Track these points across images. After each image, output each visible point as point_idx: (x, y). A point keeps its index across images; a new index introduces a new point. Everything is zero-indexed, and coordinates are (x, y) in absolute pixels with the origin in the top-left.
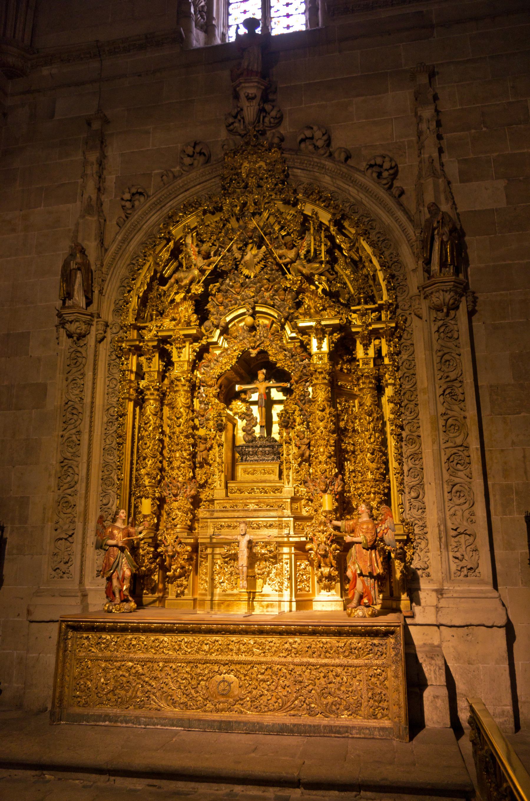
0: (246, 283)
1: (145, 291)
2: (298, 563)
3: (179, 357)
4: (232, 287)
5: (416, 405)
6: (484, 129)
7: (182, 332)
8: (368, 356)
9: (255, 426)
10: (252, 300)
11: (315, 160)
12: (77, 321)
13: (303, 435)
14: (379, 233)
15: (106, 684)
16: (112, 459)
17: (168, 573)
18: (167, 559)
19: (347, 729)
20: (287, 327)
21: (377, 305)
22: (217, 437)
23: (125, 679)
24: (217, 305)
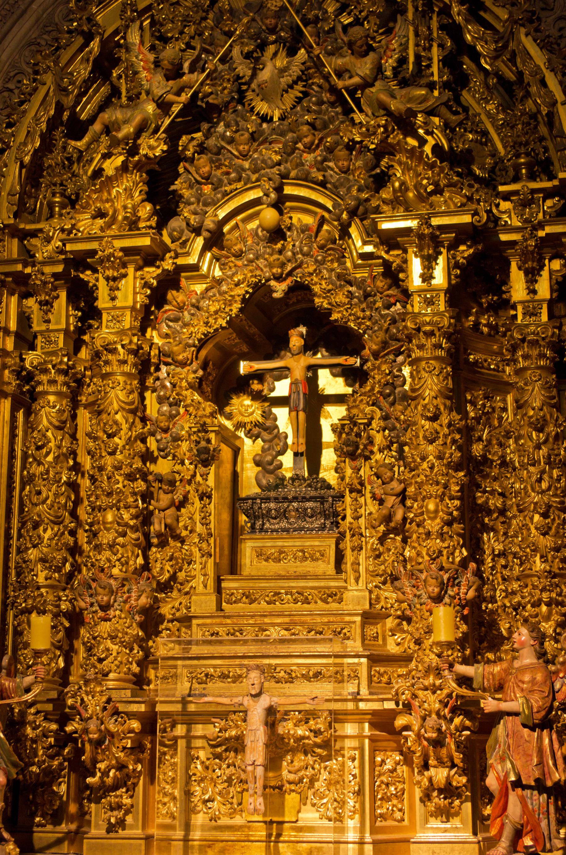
0: (262, 132)
1: (36, 151)
2: (379, 759)
3: (113, 299)
4: (231, 141)
7: (118, 244)
8: (537, 297)
9: (282, 452)
10: (275, 170)
13: (389, 474)
17: (89, 780)
18: (88, 747)
20: (353, 231)
21: (556, 182)
22: (198, 478)
24: (198, 182)
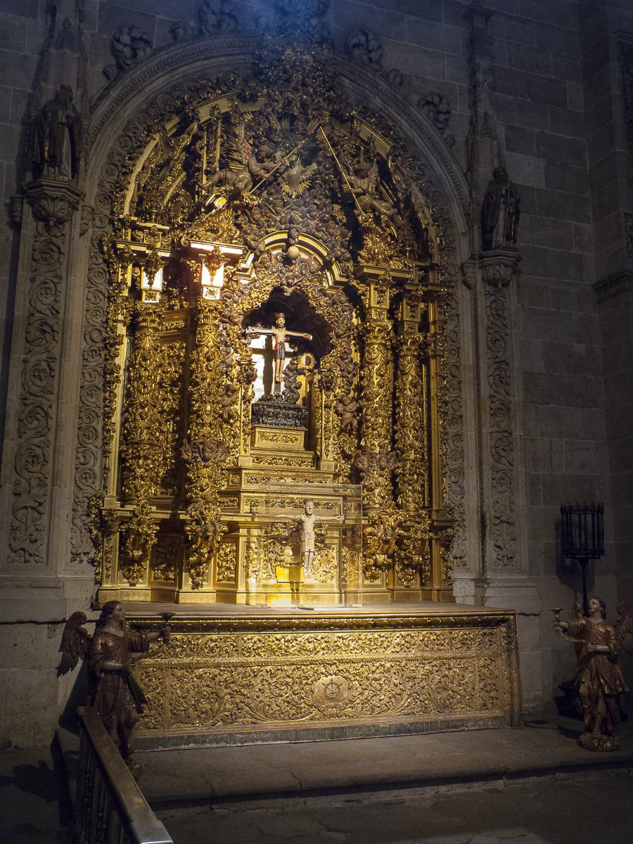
0: (288, 203)
5: (460, 383)
6: (528, 100)
8: (415, 320)
11: (370, 75)
12: (61, 200)
14: (430, 182)
15: (183, 698)
16: (96, 401)
18: (199, 539)
19: (463, 722)
20: (334, 267)
23: (209, 690)
